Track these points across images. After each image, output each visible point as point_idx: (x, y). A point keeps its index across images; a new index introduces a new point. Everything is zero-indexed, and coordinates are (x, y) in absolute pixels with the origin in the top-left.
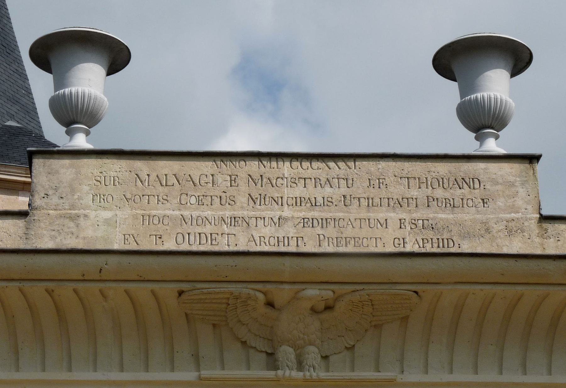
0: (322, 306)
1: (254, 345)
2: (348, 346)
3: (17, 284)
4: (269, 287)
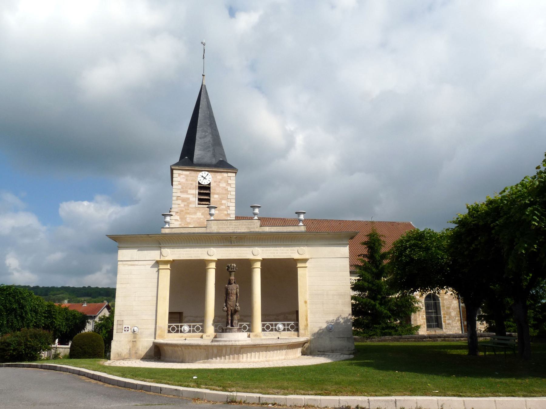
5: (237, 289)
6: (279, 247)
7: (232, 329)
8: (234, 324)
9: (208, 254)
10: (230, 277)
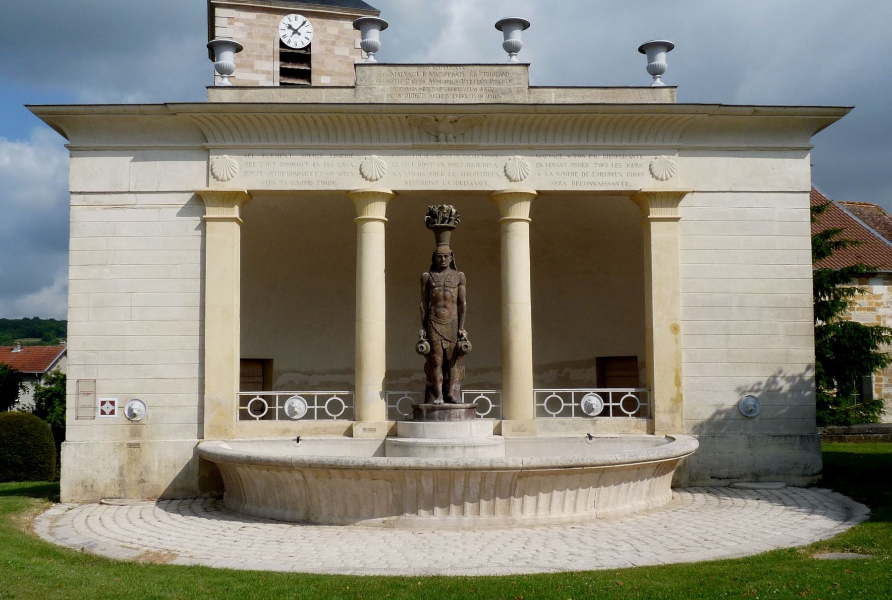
0: (453, 121)
3: (353, 114)
4: (436, 115)
5: (460, 284)
6: (589, 156)
7: (450, 408)
8: (452, 394)
9: (362, 173)
10: (438, 246)
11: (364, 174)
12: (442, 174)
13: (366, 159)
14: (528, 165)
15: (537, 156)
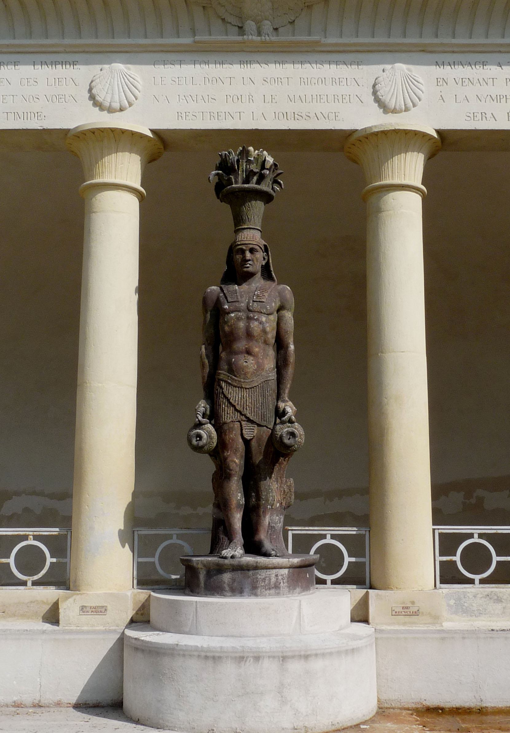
1: (229, 21)
2: (290, 21)
5: (280, 309)
7: (256, 568)
8: (263, 536)
9: (92, 97)
10: (237, 231)
11: (98, 98)
12: (251, 98)
13: (101, 70)
14: (420, 80)
15: (437, 64)
